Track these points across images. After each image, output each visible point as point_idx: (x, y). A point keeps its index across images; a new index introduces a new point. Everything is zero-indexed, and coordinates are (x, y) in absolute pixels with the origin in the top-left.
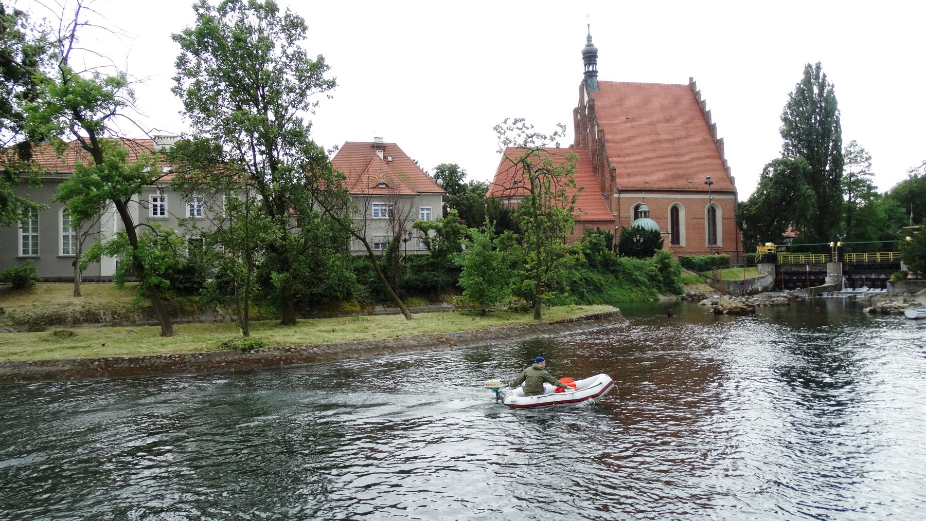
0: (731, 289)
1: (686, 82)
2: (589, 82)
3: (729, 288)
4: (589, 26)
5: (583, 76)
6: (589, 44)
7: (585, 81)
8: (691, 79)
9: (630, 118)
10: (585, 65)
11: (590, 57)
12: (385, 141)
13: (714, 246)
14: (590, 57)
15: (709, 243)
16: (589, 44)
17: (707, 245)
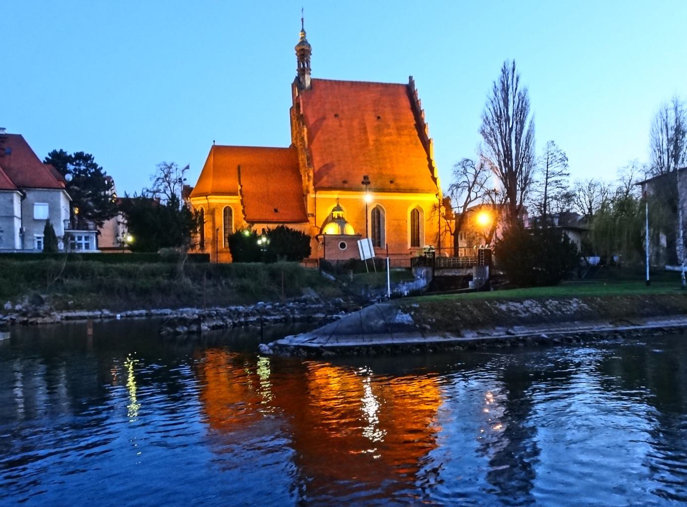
0: (363, 293)
1: (407, 82)
2: (301, 80)
3: (361, 292)
4: (302, 19)
5: (296, 74)
6: (303, 42)
7: (297, 79)
8: (411, 78)
9: (341, 116)
10: (298, 62)
11: (303, 53)
12: (7, 132)
13: (416, 248)
14: (303, 53)
15: (413, 244)
16: (303, 42)
17: (409, 246)
